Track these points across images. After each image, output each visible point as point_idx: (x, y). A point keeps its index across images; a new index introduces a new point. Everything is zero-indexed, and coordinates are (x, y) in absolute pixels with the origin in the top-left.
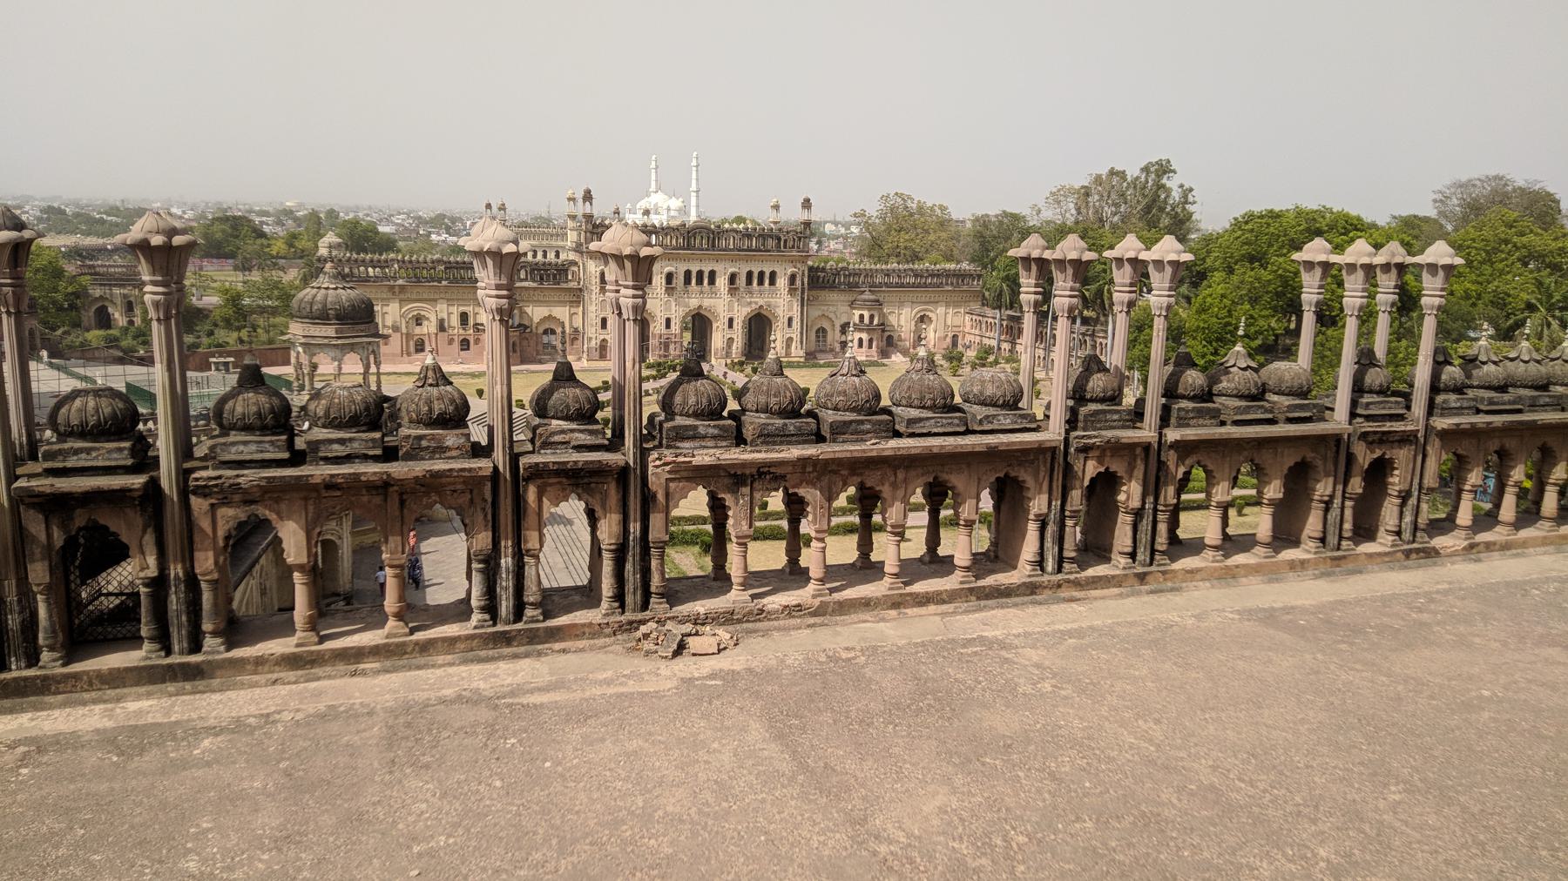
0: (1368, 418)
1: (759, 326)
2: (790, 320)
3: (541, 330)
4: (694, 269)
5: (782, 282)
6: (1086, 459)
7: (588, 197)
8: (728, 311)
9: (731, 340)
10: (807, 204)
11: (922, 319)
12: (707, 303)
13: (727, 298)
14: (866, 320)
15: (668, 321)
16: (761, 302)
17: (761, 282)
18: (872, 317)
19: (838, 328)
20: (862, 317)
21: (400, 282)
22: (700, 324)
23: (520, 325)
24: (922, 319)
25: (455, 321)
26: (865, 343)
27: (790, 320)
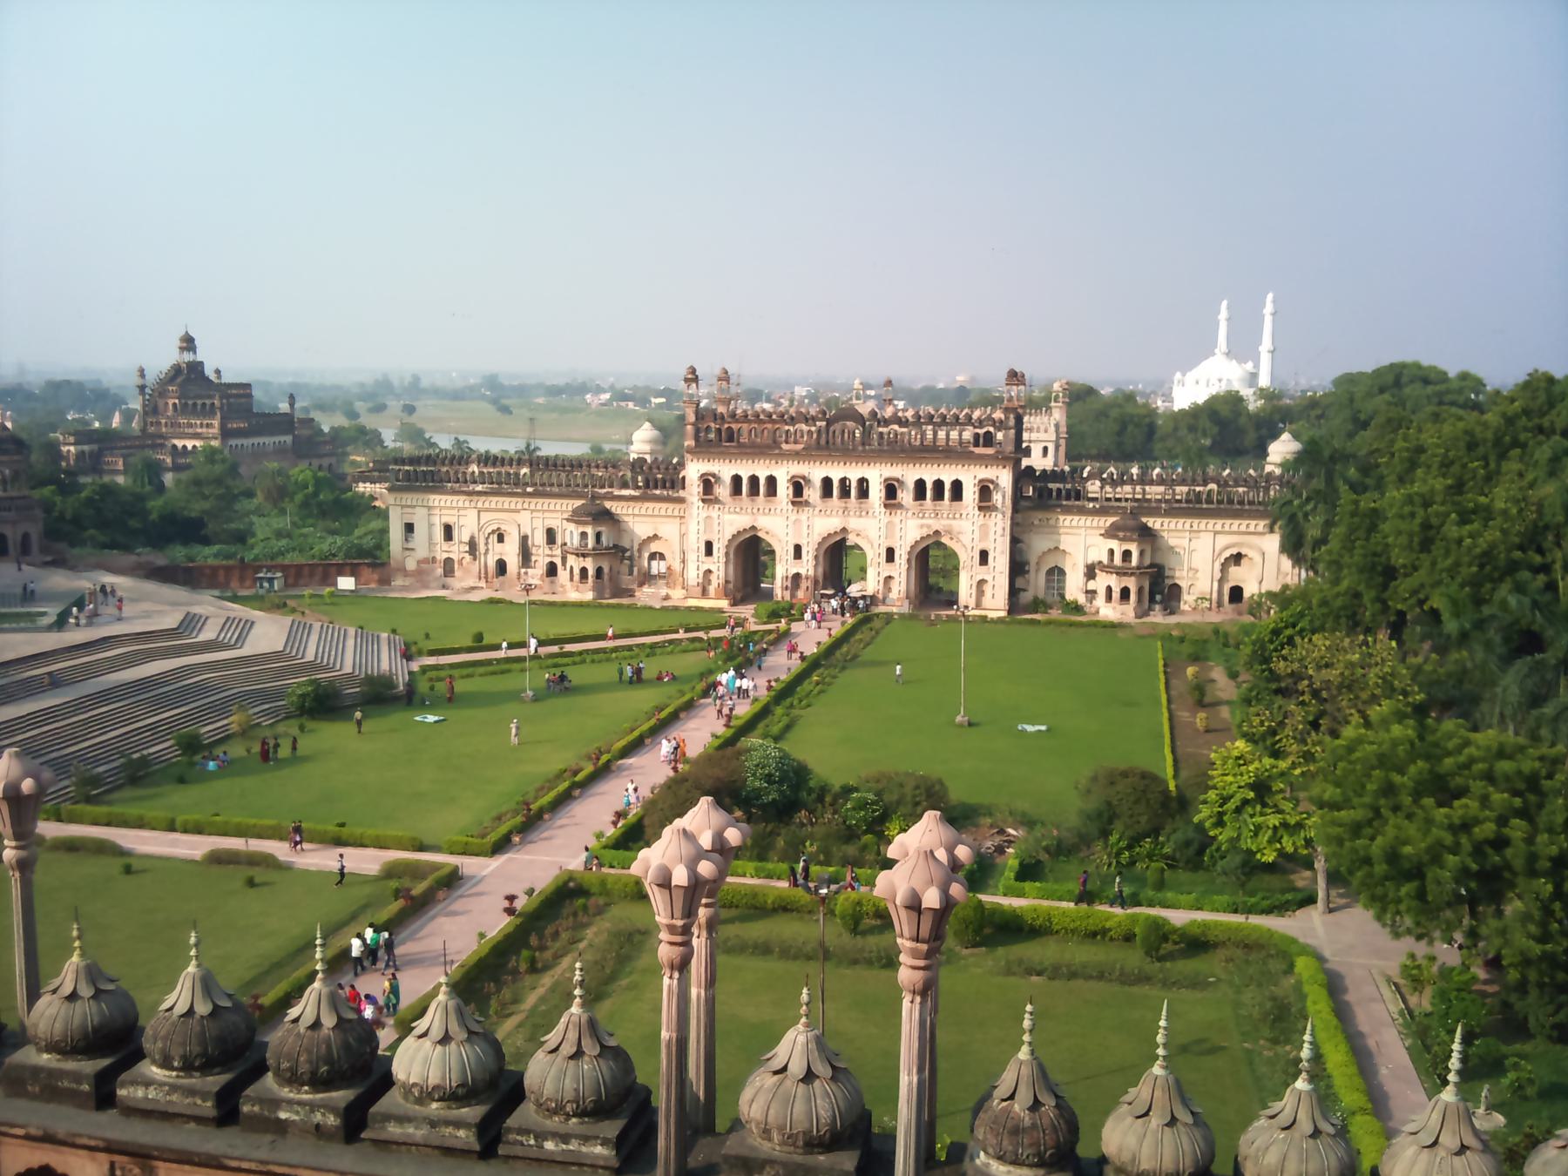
2: (984, 556)
5: (970, 493)
8: (884, 536)
11: (1237, 558)
12: (854, 523)
14: (1118, 560)
16: (936, 525)
18: (1127, 555)
19: (1081, 570)
20: (1111, 552)
21: (479, 488)
23: (615, 546)
24: (1237, 558)
25: (539, 538)
26: (1116, 594)
27: (984, 556)
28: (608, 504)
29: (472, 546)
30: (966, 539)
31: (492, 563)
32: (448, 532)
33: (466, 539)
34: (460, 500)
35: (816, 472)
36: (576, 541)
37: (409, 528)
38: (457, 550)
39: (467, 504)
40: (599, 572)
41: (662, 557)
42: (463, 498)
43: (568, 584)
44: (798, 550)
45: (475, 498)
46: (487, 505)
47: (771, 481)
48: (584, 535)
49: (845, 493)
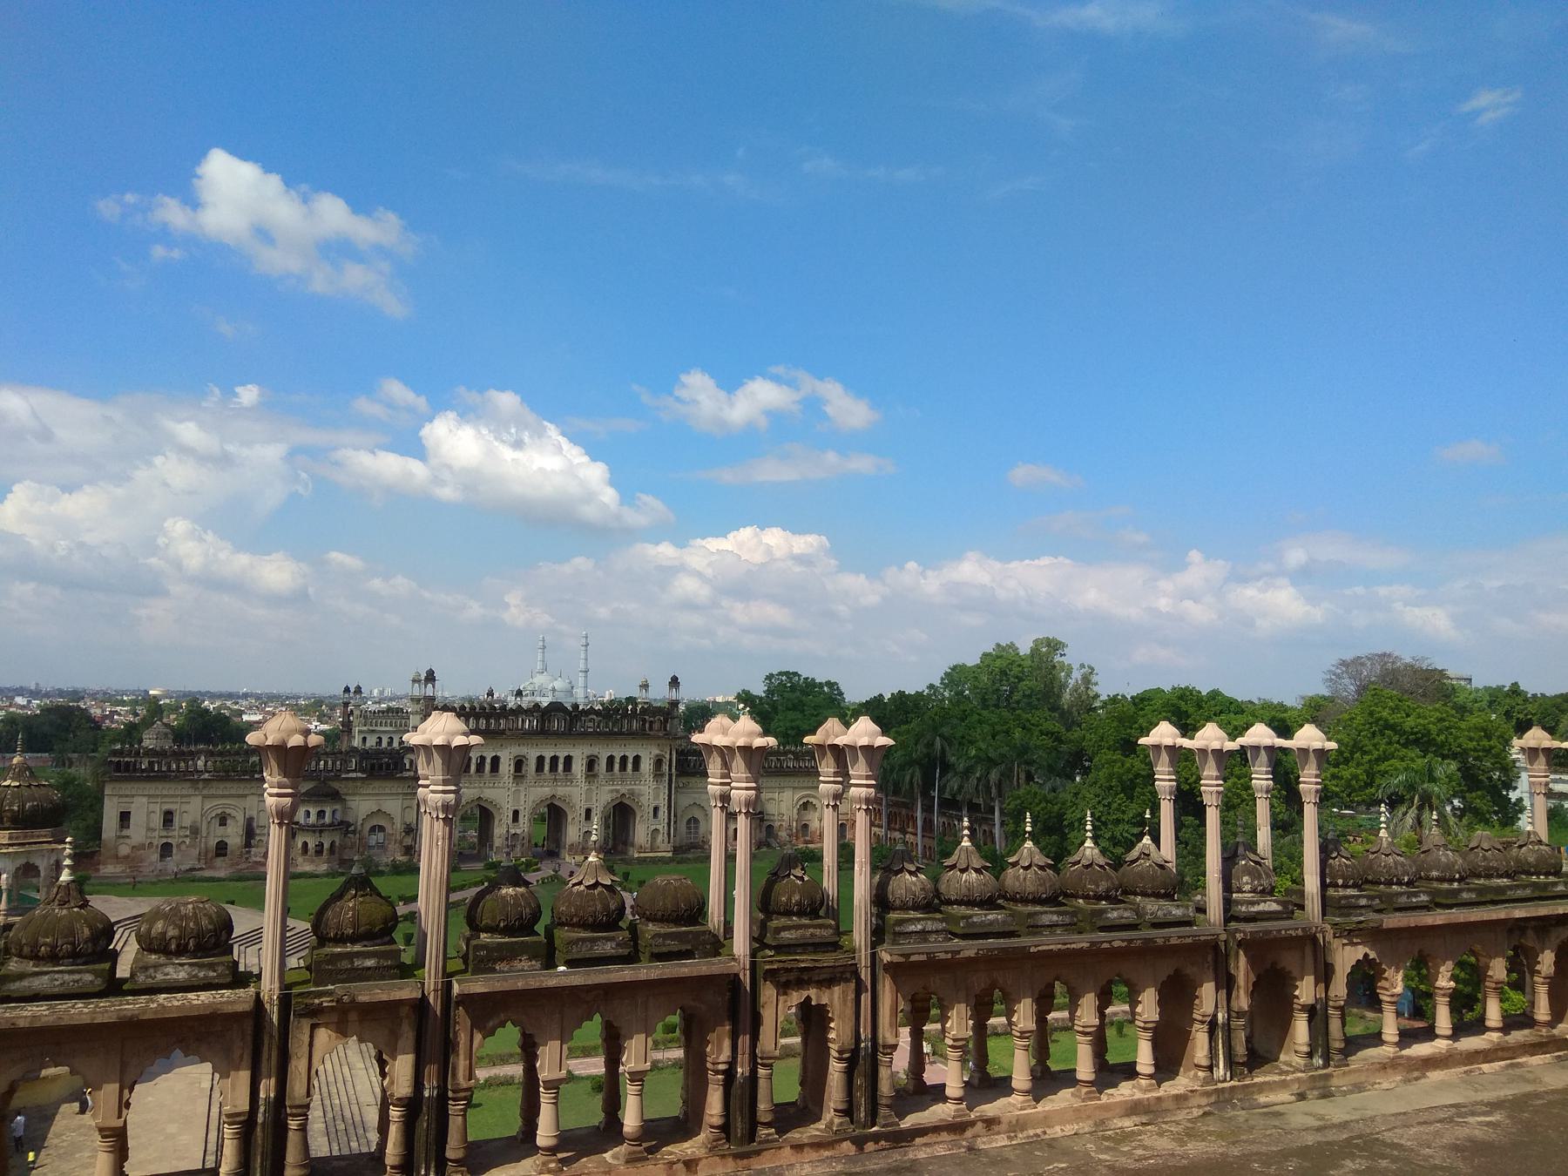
0: (780, 948)
1: (621, 815)
2: (656, 809)
3: (367, 827)
4: (548, 755)
5: (647, 766)
6: (314, 1027)
7: (430, 677)
9: (588, 833)
10: (674, 682)
11: (805, 806)
12: (561, 791)
13: (584, 786)
15: (516, 813)
17: (623, 767)
21: (206, 776)
22: (554, 815)
23: (342, 823)
24: (805, 806)
27: (656, 809)
28: (336, 785)
29: (195, 831)
30: (644, 800)
31: (213, 842)
32: (168, 818)
33: (187, 823)
34: (185, 789)
35: (532, 753)
36: (313, 819)
37: (125, 817)
38: (175, 836)
39: (191, 791)
40: (332, 844)
41: (381, 829)
42: (188, 784)
43: (300, 860)
44: (516, 813)
45: (201, 785)
46: (213, 791)
47: (496, 760)
48: (321, 814)
49: (554, 767)
